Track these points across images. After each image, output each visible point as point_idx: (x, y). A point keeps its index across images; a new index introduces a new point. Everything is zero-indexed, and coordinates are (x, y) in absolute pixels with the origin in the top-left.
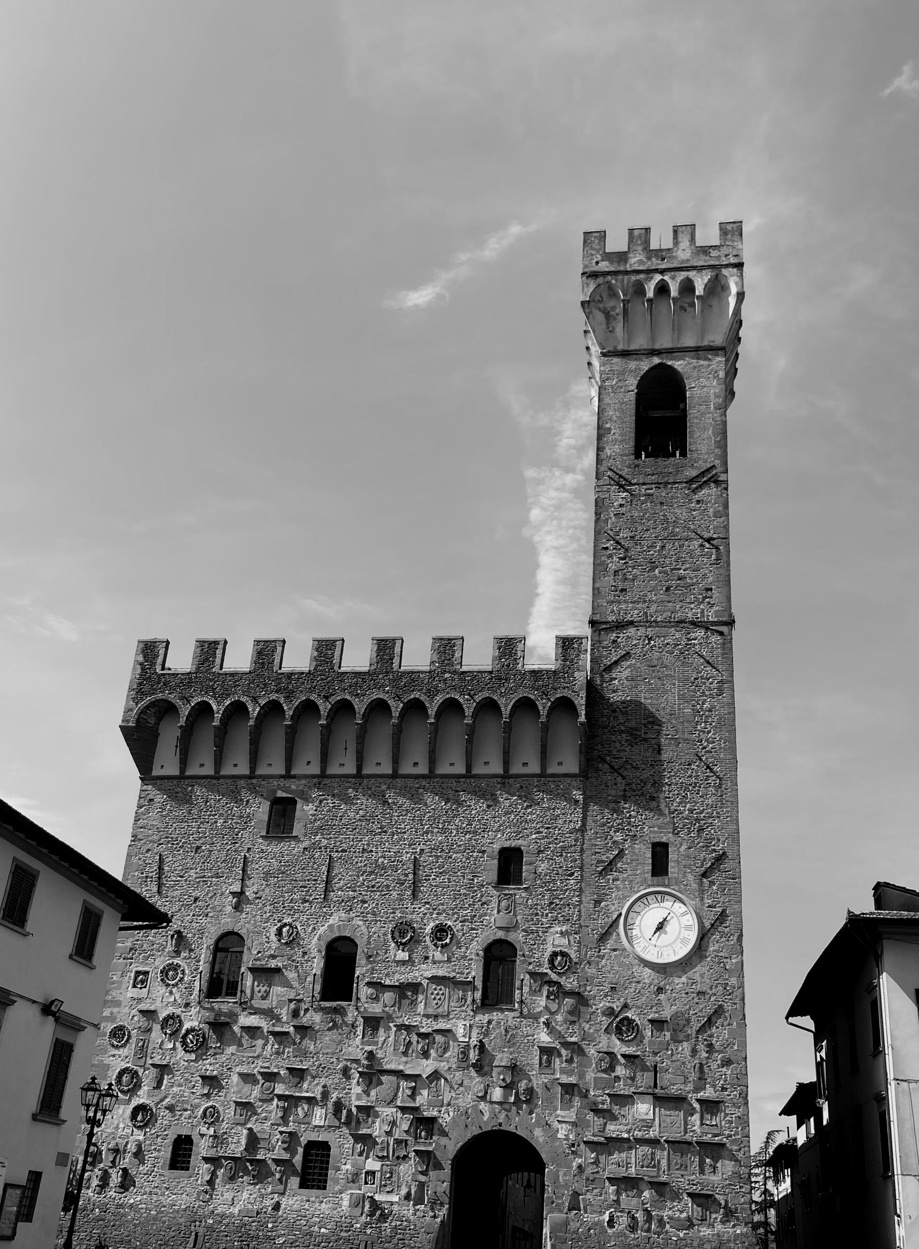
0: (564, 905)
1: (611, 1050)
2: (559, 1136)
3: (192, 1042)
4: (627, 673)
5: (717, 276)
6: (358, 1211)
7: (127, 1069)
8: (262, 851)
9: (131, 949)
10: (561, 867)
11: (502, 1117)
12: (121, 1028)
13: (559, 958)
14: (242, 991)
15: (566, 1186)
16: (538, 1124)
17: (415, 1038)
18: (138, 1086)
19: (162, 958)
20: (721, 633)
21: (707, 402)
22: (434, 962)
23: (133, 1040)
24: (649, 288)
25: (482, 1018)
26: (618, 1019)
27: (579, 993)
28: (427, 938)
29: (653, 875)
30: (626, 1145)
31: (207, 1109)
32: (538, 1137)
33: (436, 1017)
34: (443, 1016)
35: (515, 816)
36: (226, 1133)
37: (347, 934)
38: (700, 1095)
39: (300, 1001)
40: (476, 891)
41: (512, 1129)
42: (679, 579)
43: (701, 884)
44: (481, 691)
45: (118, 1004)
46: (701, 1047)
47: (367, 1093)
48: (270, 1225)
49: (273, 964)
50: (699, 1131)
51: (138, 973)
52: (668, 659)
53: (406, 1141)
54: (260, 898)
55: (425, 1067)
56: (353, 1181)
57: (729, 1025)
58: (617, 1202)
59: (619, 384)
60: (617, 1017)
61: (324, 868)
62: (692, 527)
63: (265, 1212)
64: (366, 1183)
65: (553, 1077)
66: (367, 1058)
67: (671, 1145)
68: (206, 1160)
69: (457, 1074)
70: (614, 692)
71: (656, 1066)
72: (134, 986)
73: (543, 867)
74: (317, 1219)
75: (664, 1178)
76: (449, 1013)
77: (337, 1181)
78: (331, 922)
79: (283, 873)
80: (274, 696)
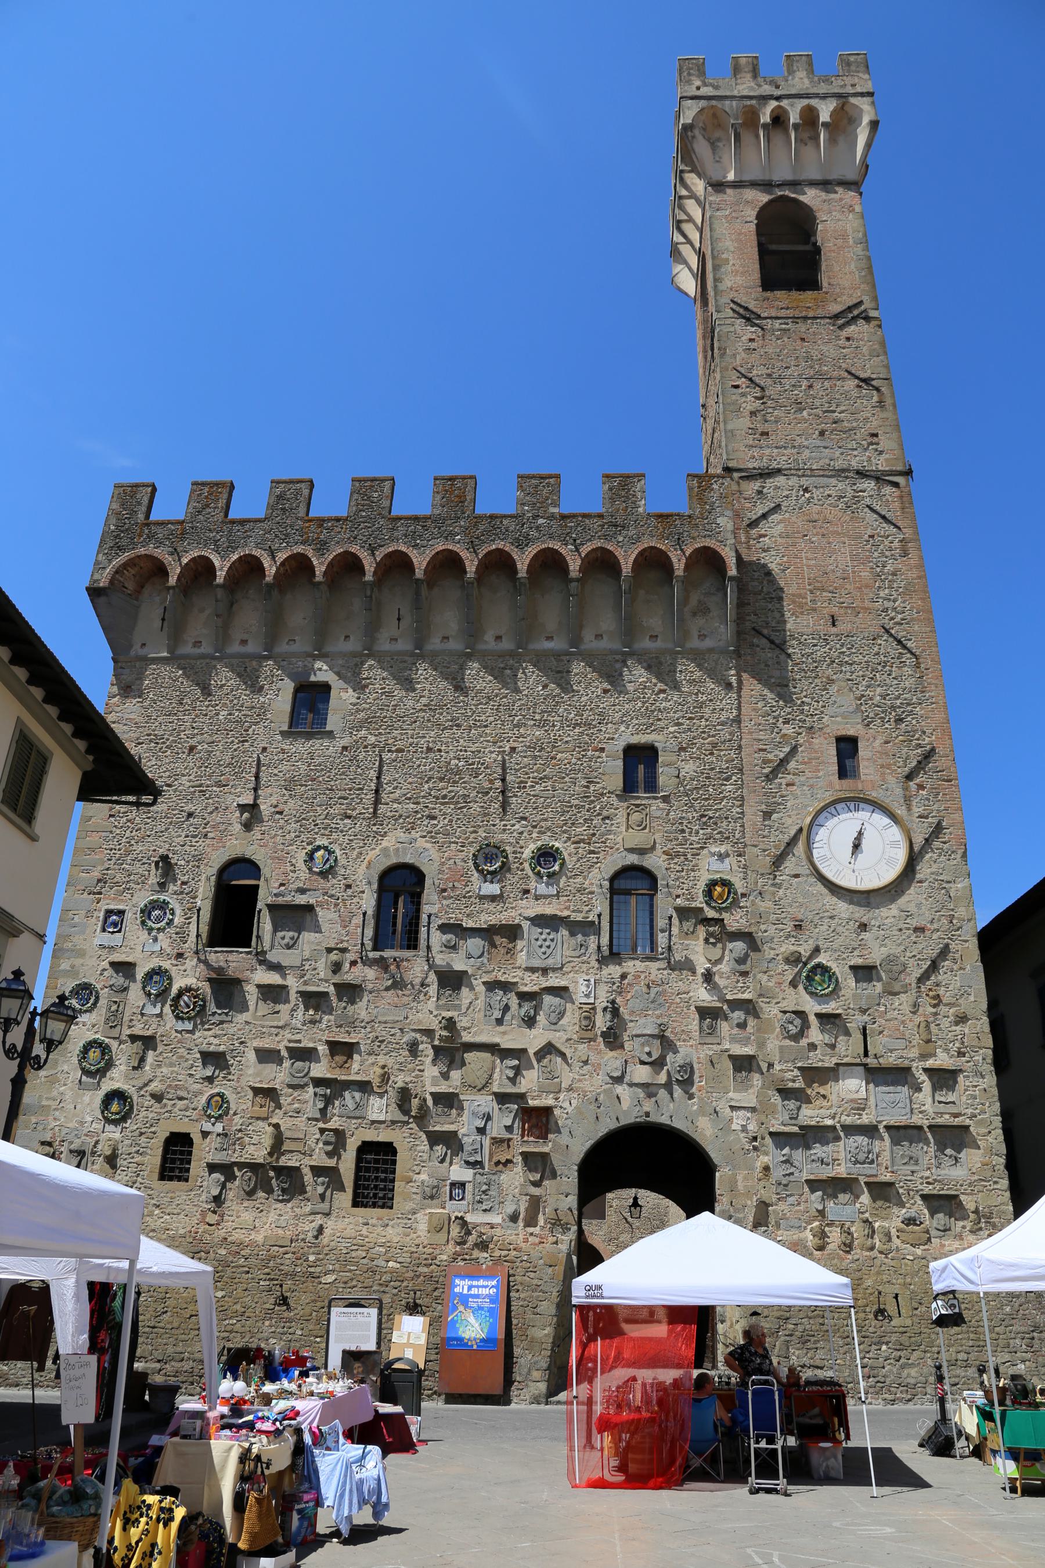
0: (720, 817)
1: (800, 1009)
2: (734, 1127)
3: (188, 1006)
4: (780, 528)
5: (843, 105)
6: (442, 1237)
7: (95, 1041)
8: (283, 751)
9: (99, 881)
10: (712, 769)
11: (648, 1106)
12: (86, 987)
13: (718, 889)
14: (258, 937)
15: (748, 1194)
16: (702, 1111)
17: (514, 1001)
18: (110, 1065)
19: (143, 892)
20: (896, 485)
21: (844, 237)
22: (537, 898)
23: (103, 1002)
24: (764, 114)
25: (614, 970)
26: (809, 966)
27: (750, 934)
28: (526, 865)
29: (840, 778)
30: (830, 1135)
31: (212, 1096)
32: (704, 1131)
33: (545, 971)
34: (554, 970)
35: (644, 703)
36: (240, 1130)
37: (408, 859)
38: (930, 1063)
39: (344, 950)
40: (593, 802)
41: (664, 1120)
42: (835, 423)
43: (906, 789)
44: (590, 540)
45: (81, 953)
46: (924, 1001)
47: (445, 1076)
48: (312, 1258)
49: (301, 900)
50: (931, 1111)
51: (109, 913)
52: (833, 514)
53: (509, 1140)
54: (281, 813)
55: (532, 1040)
56: (432, 1197)
57: (961, 969)
58: (822, 1213)
59: (733, 214)
60: (805, 964)
61: (373, 774)
62: (844, 365)
63: (303, 1240)
64: (451, 1198)
65: (720, 1047)
66: (445, 1028)
67: (893, 1132)
68: (212, 1168)
69: (581, 1047)
70: (764, 551)
71: (864, 1029)
72: (104, 930)
73: (689, 768)
74: (381, 1249)
75: (886, 1177)
76: (563, 965)
77: (407, 1198)
78: (385, 844)
79: (313, 780)
80: (299, 549)
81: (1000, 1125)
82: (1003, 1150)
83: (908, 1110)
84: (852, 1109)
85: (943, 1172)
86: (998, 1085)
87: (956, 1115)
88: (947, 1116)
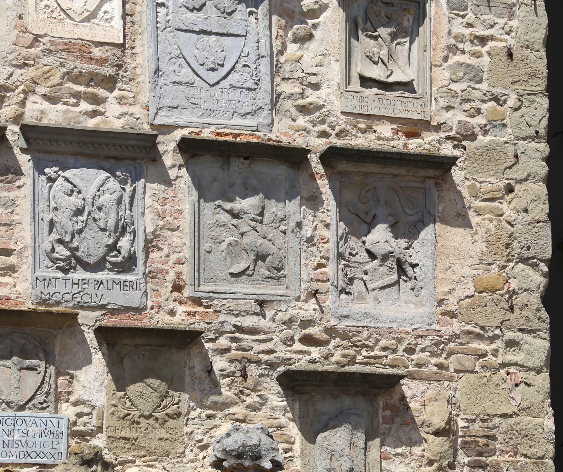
67: (209, 166)
81: (543, 170)
82: (543, 243)
83: (263, 97)
84: (69, 76)
85: (356, 308)
86: (551, 43)
87: (413, 128)
88: (385, 130)
